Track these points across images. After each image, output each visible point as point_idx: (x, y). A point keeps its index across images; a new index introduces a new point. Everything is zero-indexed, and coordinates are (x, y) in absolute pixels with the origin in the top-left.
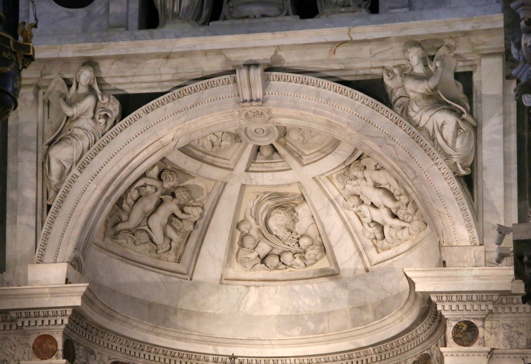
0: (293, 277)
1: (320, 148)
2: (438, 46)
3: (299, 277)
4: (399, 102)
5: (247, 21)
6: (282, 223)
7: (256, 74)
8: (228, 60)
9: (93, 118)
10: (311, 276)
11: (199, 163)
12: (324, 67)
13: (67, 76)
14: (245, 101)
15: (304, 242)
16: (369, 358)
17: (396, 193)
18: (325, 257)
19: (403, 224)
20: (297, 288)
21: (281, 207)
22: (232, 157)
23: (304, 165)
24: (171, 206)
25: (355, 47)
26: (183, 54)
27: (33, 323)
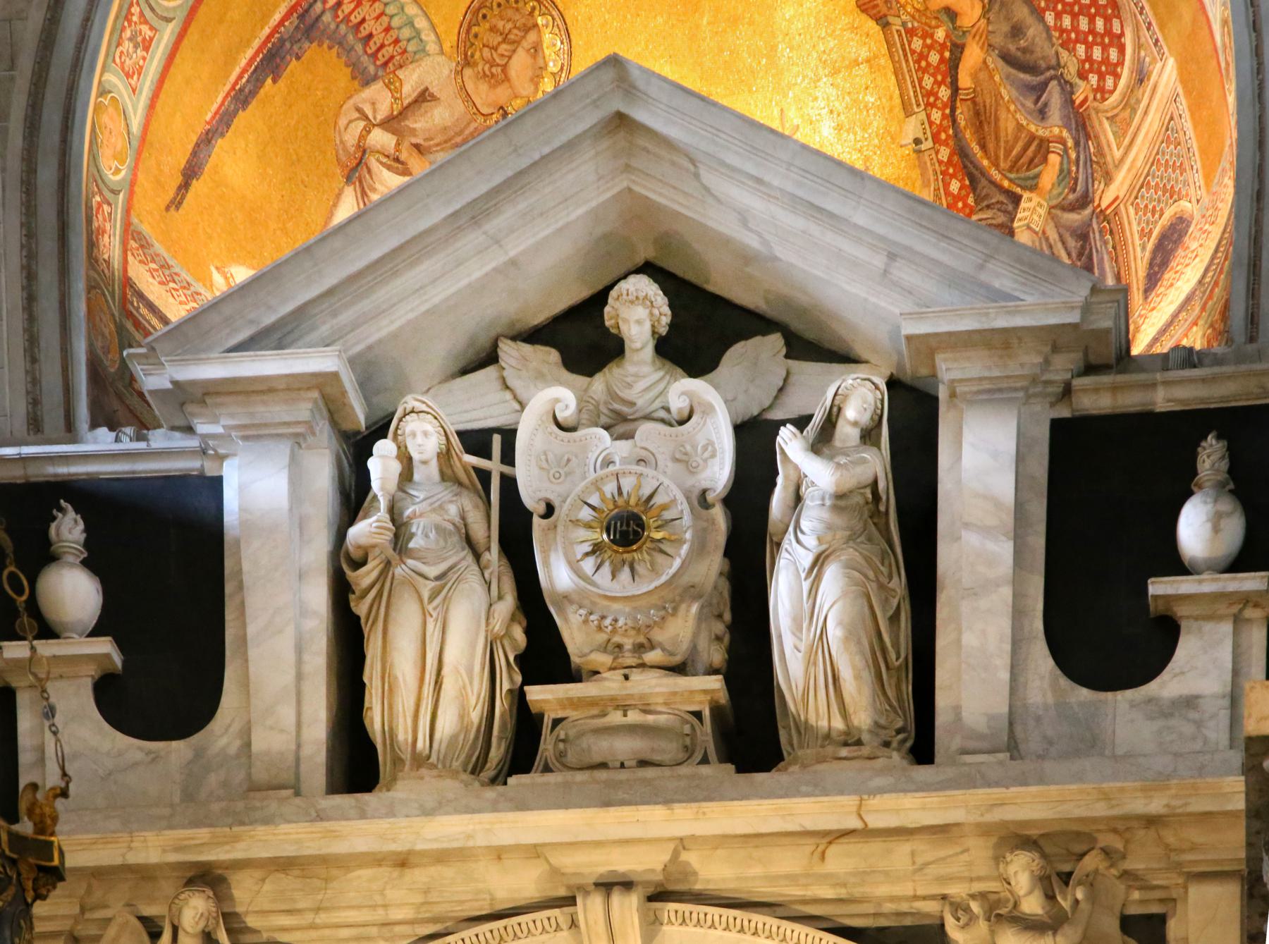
2: (1078, 848)
5: (602, 775)
7: (627, 907)
8: (555, 872)
12: (796, 892)
13: (148, 911)
25: (876, 846)
26: (442, 857)
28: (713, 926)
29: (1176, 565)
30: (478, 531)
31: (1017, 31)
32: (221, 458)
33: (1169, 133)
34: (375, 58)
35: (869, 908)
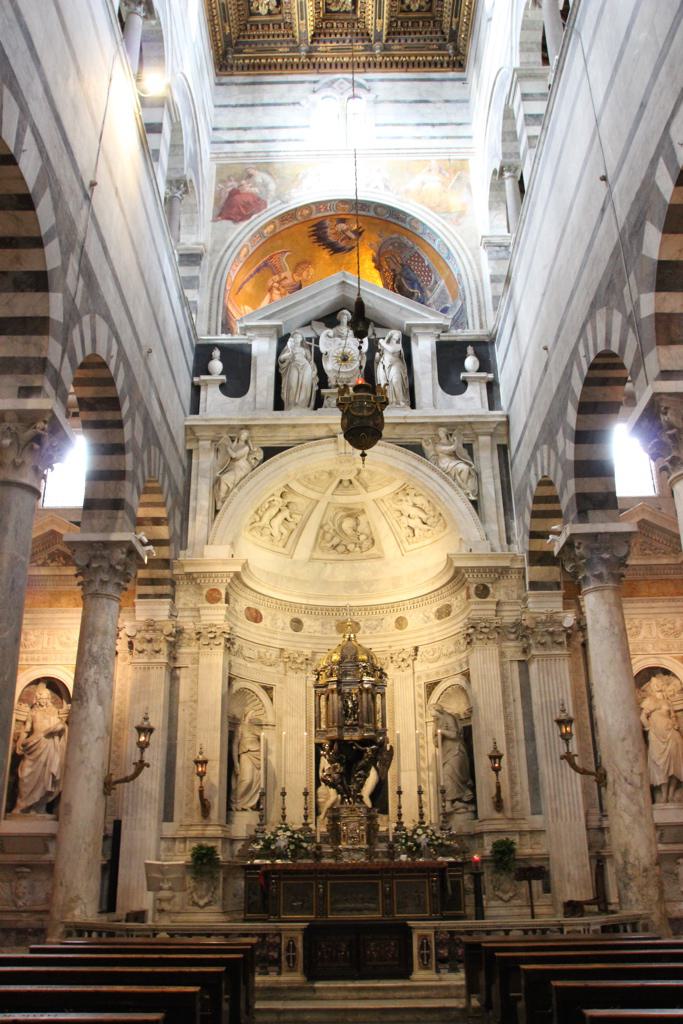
15: (362, 537)
17: (426, 510)
20: (356, 564)
21: (349, 516)
24: (286, 513)
29: (466, 371)
30: (309, 357)
31: (408, 274)
32: (251, 340)
33: (443, 292)
34: (276, 271)
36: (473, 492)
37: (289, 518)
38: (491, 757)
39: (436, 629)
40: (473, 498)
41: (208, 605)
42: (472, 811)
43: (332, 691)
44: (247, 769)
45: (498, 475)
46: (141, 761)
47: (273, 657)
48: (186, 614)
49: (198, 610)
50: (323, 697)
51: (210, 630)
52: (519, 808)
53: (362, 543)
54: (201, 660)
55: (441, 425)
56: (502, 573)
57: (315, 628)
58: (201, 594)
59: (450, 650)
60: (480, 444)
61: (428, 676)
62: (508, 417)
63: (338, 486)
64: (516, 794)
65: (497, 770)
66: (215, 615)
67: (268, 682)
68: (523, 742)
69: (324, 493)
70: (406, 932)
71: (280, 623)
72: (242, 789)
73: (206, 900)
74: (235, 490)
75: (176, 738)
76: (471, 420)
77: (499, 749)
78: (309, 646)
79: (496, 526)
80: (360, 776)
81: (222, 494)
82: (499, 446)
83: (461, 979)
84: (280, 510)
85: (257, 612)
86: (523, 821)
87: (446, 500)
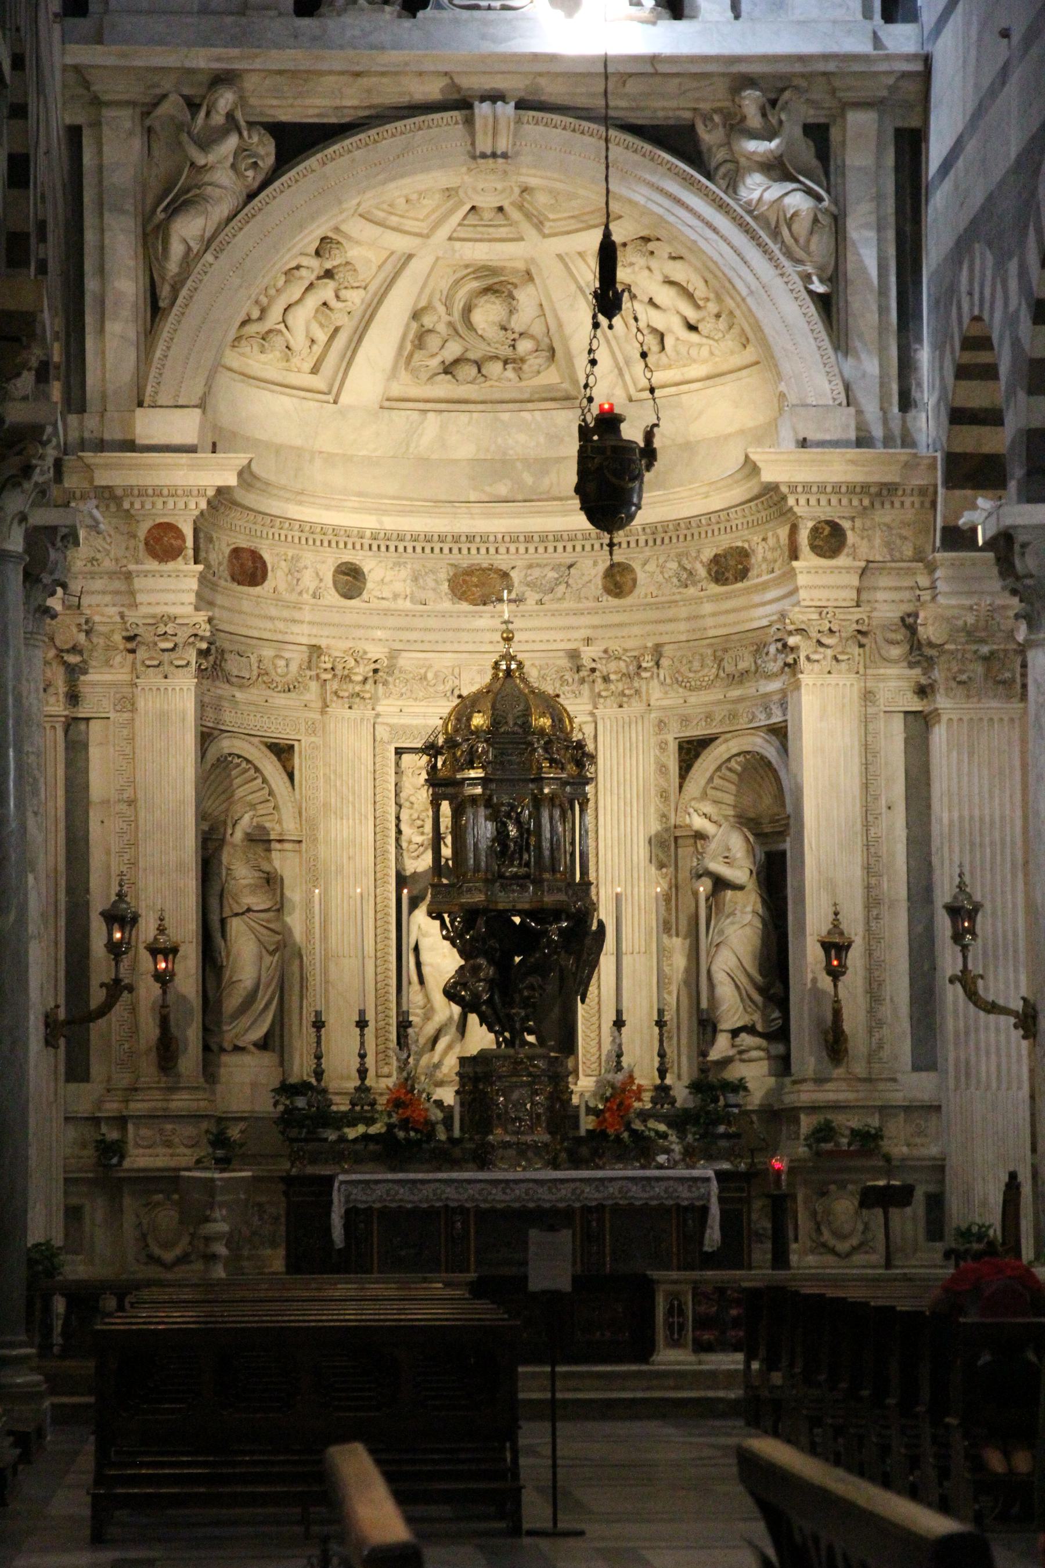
0: (497, 396)
1: (576, 213)
3: (507, 396)
4: (722, 170)
6: (497, 319)
9: (233, 166)
10: (526, 396)
11: (381, 229)
14: (484, 156)
15: (524, 346)
16: (632, 540)
17: (697, 294)
18: (553, 368)
19: (705, 340)
20: (505, 416)
21: (487, 290)
22: (428, 216)
23: (545, 236)
24: (326, 291)
27: (148, 506)
28: (555, 127)
35: (648, 113)
36: (821, 269)
37: (333, 303)
38: (827, 946)
39: (708, 608)
40: (819, 288)
41: (153, 565)
42: (777, 1057)
43: (474, 800)
44: (246, 955)
45: (892, 220)
46: (117, 981)
47: (294, 668)
48: (98, 584)
49: (128, 576)
50: (445, 807)
51: (161, 630)
52: (885, 1054)
53: (523, 360)
54: (141, 704)
55: (747, 81)
56: (879, 494)
57: (399, 587)
58: (134, 536)
59: (743, 665)
60: (850, 134)
61: (685, 720)
62: (927, 60)
63: (465, 218)
64: (880, 1024)
65: (835, 974)
66: (173, 591)
67: (283, 733)
68: (903, 906)
69: (427, 236)
70: (646, 1288)
71: (308, 580)
72: (232, 1002)
73: (178, 1251)
74: (209, 257)
75: (87, 891)
76: (831, 67)
77: (844, 926)
78: (379, 634)
79: (870, 366)
80: (532, 987)
81: (173, 267)
82: (899, 133)
83: (737, 1363)
84: (311, 286)
85: (256, 556)
86: (890, 1085)
87: (752, 292)
